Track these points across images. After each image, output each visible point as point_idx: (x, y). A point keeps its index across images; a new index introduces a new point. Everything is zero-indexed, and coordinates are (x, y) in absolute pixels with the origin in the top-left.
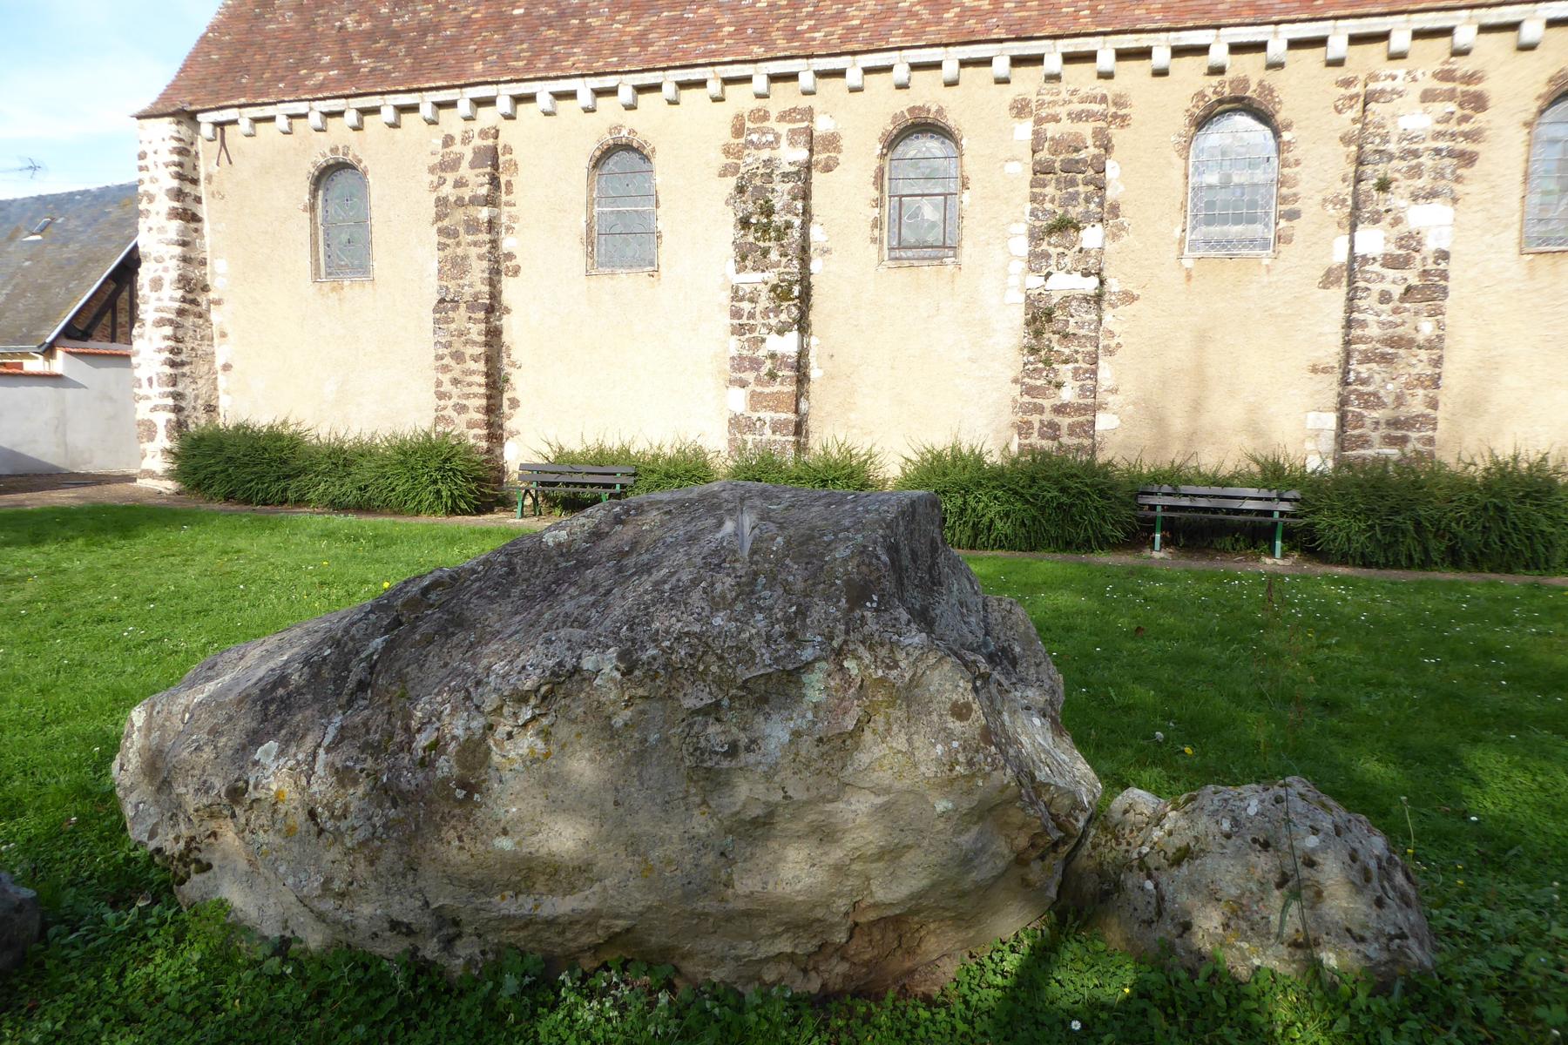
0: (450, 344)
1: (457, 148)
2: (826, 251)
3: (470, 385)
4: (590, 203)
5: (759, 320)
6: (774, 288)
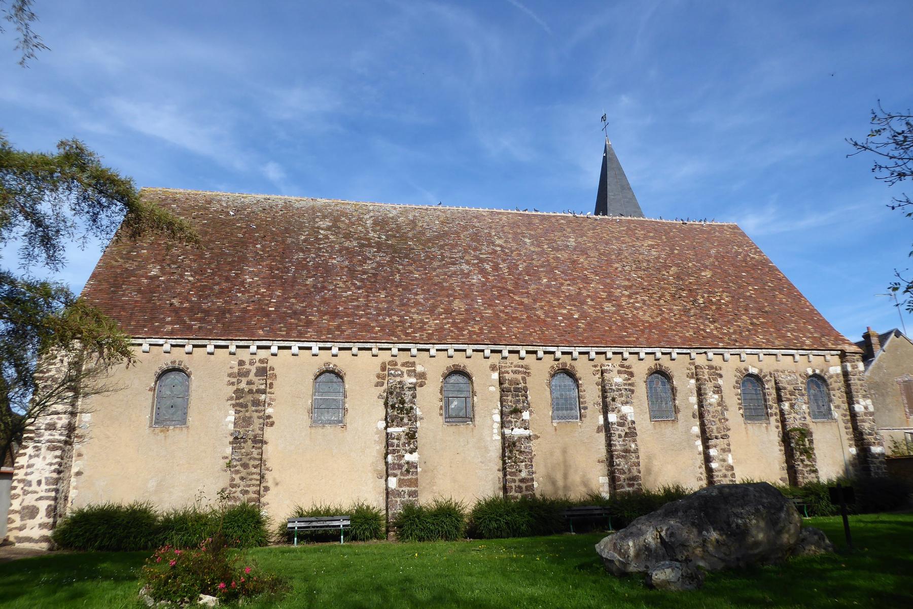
0: (241, 460)
1: (247, 366)
2: (421, 419)
3: (251, 480)
4: (314, 394)
5: (401, 447)
6: (407, 434)
